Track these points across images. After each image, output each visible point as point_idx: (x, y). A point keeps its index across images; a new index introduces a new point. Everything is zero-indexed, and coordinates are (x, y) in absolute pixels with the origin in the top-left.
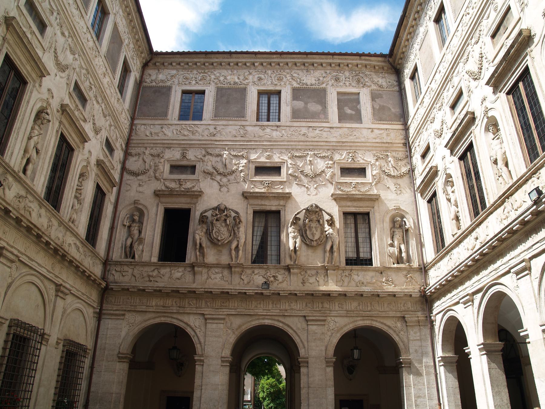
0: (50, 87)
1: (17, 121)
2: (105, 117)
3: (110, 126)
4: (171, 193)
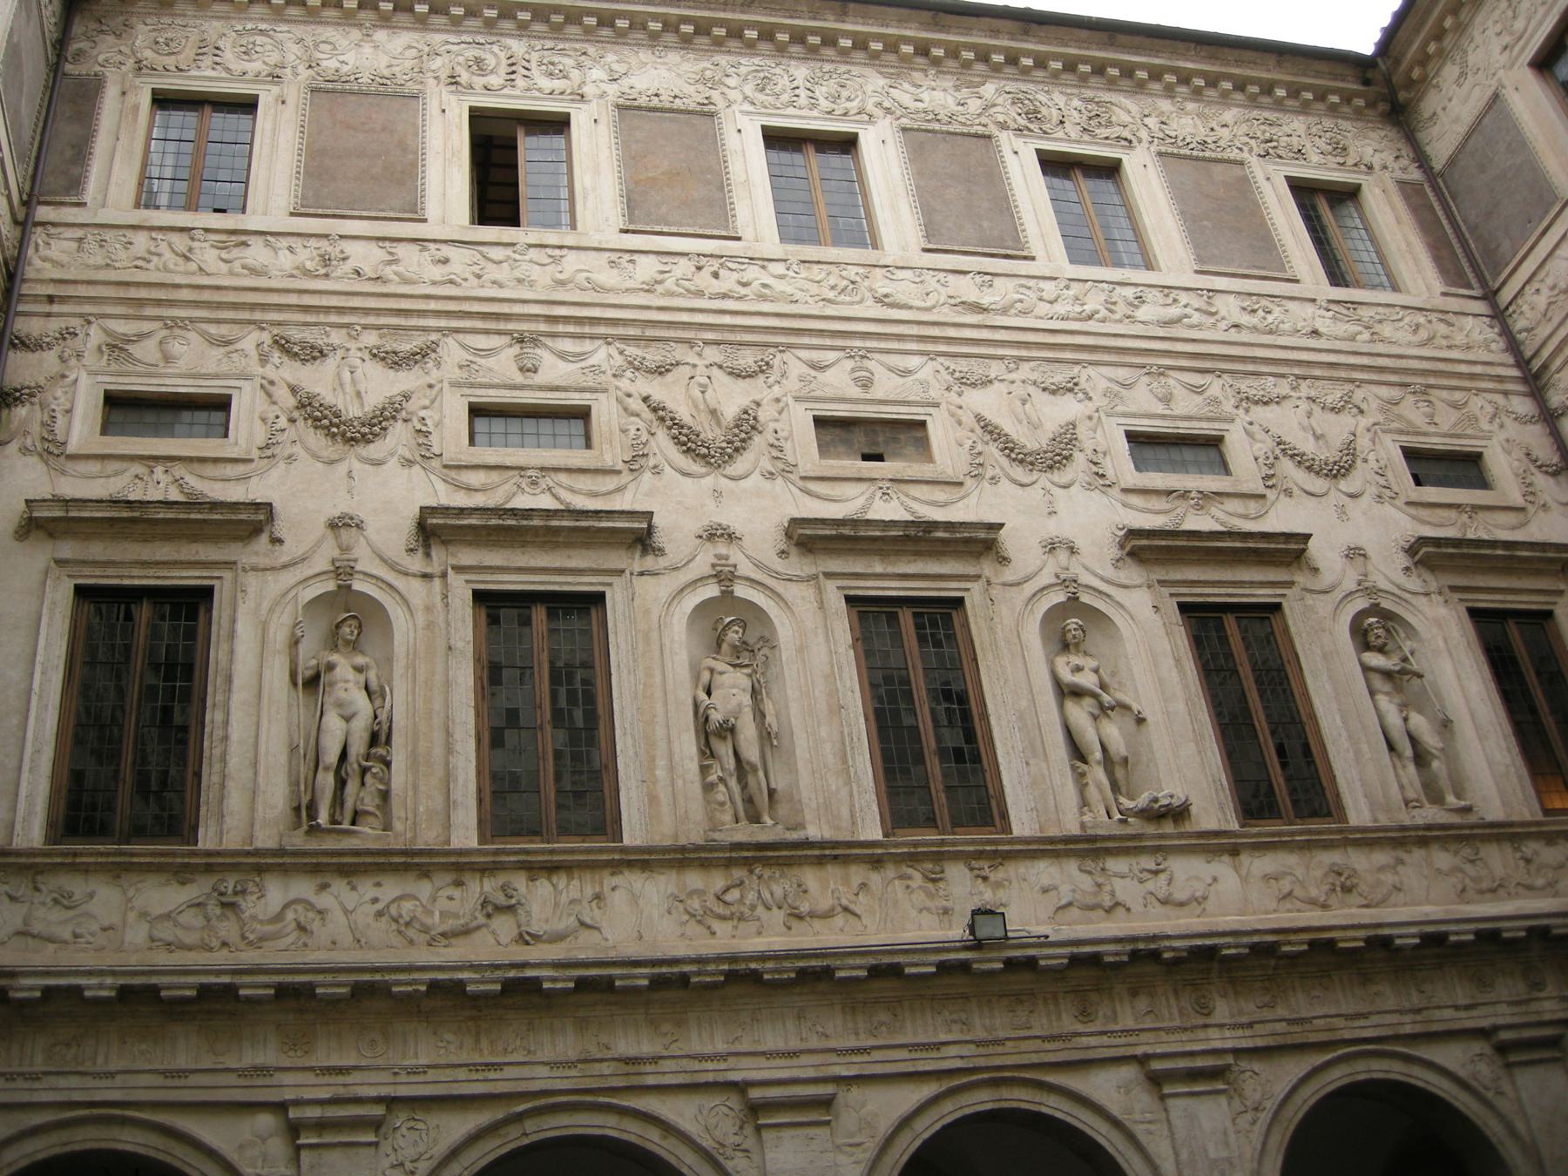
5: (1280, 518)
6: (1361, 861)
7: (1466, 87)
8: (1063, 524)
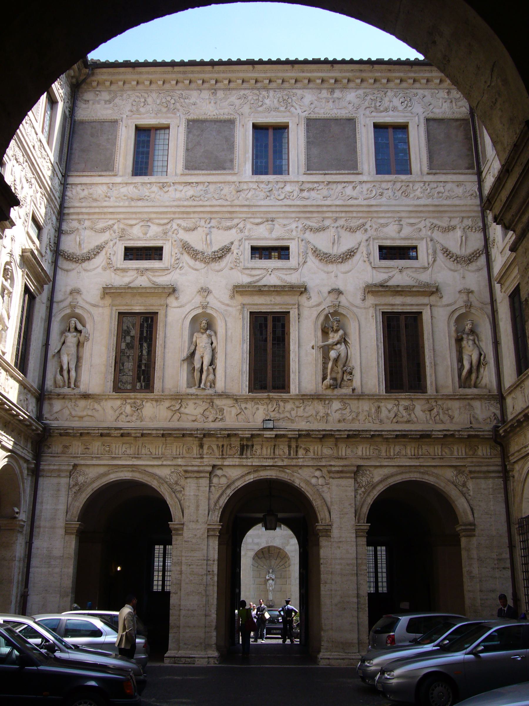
4: (127, 291)
7: (107, 106)
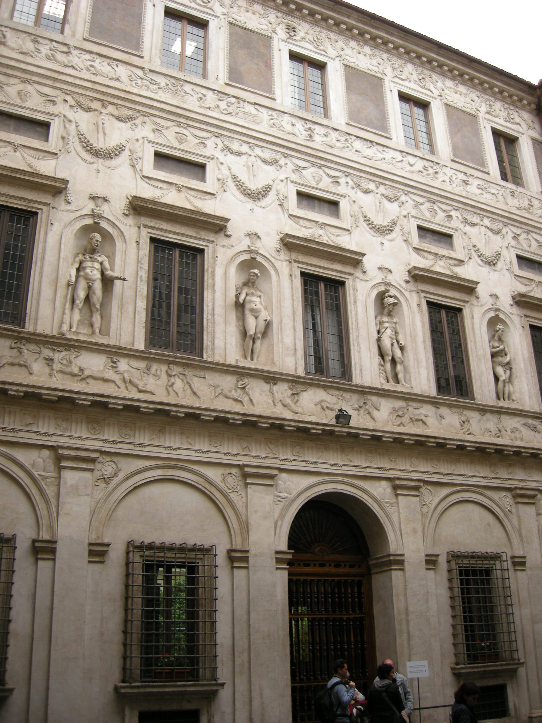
0: (379, 265)
1: (351, 331)
2: (497, 232)
3: (515, 237)
5: (467, 272)
6: (474, 416)
8: (386, 259)
